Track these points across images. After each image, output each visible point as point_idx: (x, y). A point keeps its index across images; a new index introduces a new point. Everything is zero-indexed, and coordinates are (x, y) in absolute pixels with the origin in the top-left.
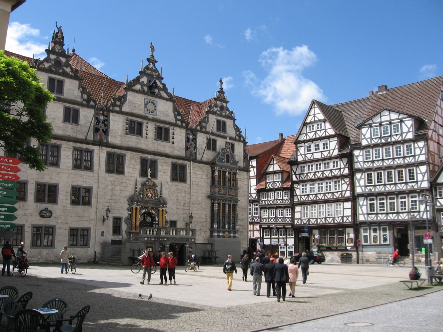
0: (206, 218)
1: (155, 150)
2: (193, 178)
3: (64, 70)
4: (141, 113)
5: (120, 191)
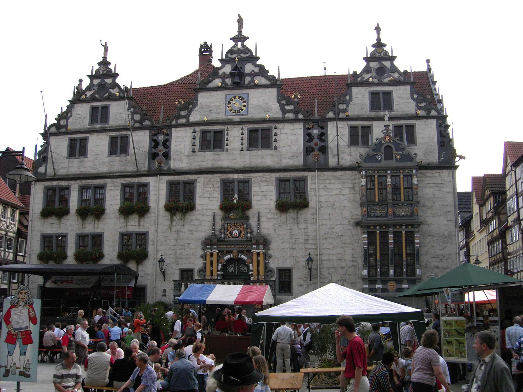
0: (354, 259)
1: (246, 165)
2: (323, 196)
3: (110, 93)
4: (222, 116)
5: (189, 232)
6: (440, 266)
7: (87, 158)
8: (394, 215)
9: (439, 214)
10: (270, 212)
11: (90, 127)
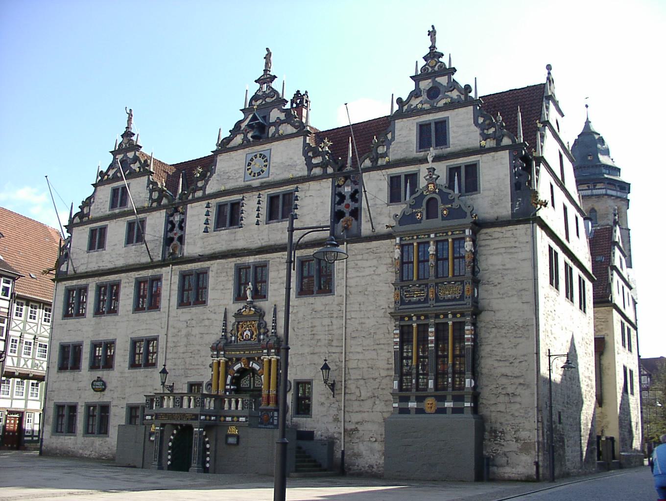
1: (264, 244)
4: (241, 183)
5: (200, 336)
6: (510, 374)
7: (105, 250)
8: (437, 299)
9: (510, 293)
11: (110, 212)
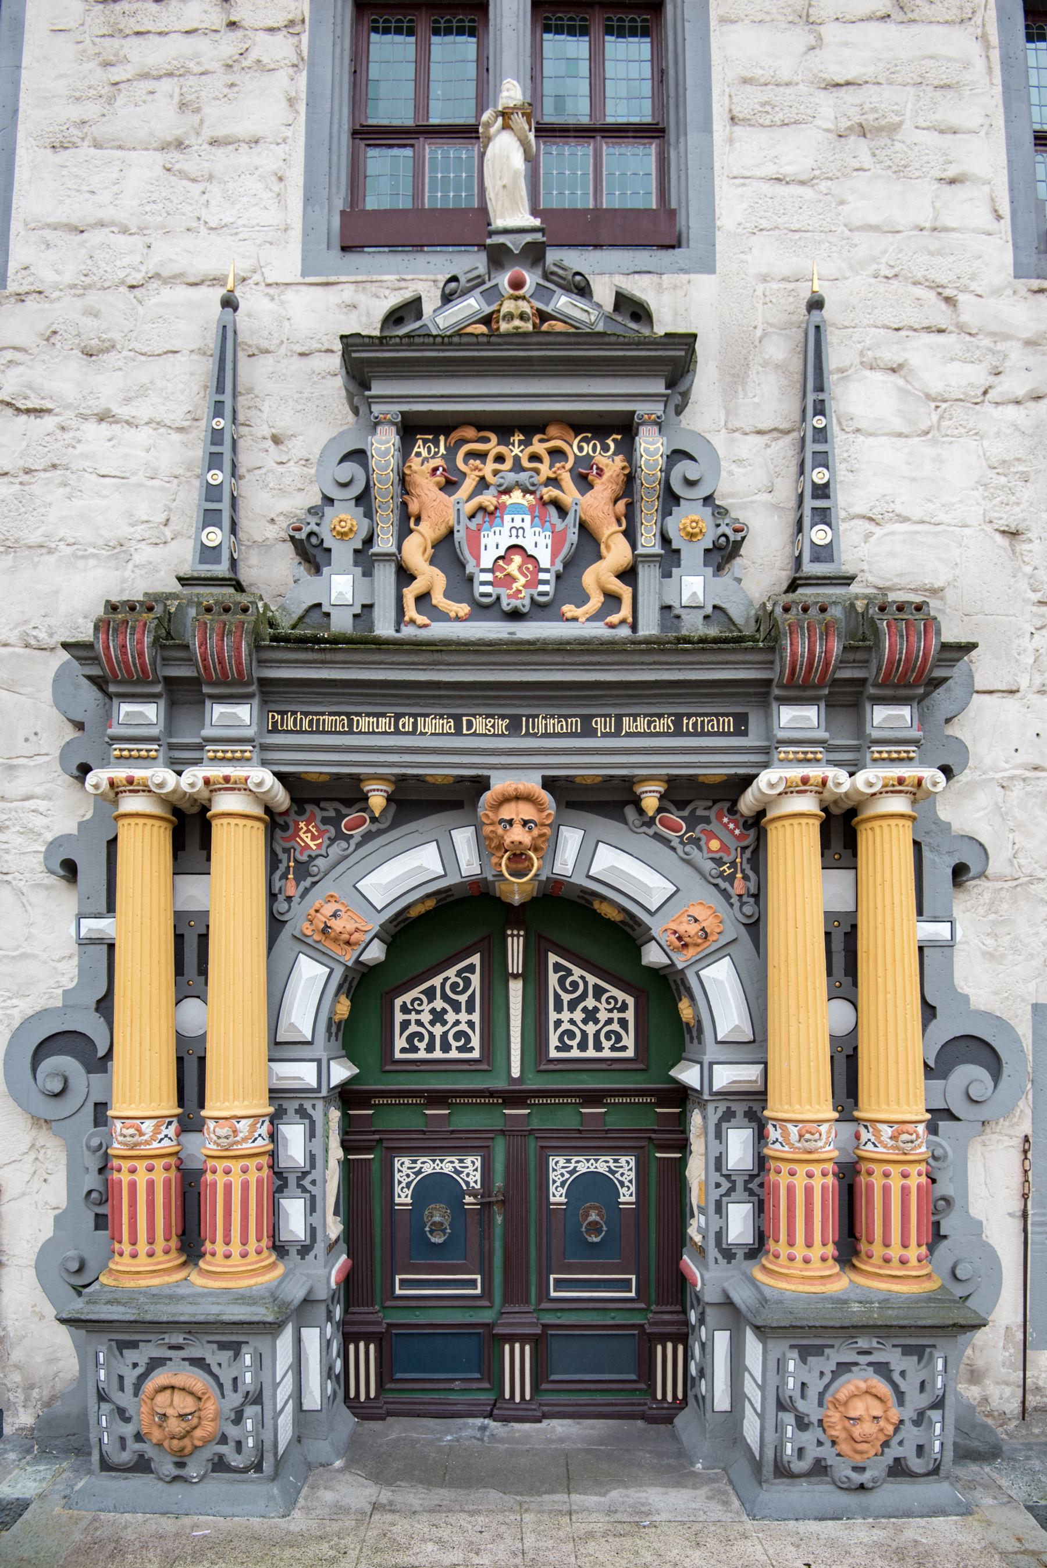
10: (941, 316)
